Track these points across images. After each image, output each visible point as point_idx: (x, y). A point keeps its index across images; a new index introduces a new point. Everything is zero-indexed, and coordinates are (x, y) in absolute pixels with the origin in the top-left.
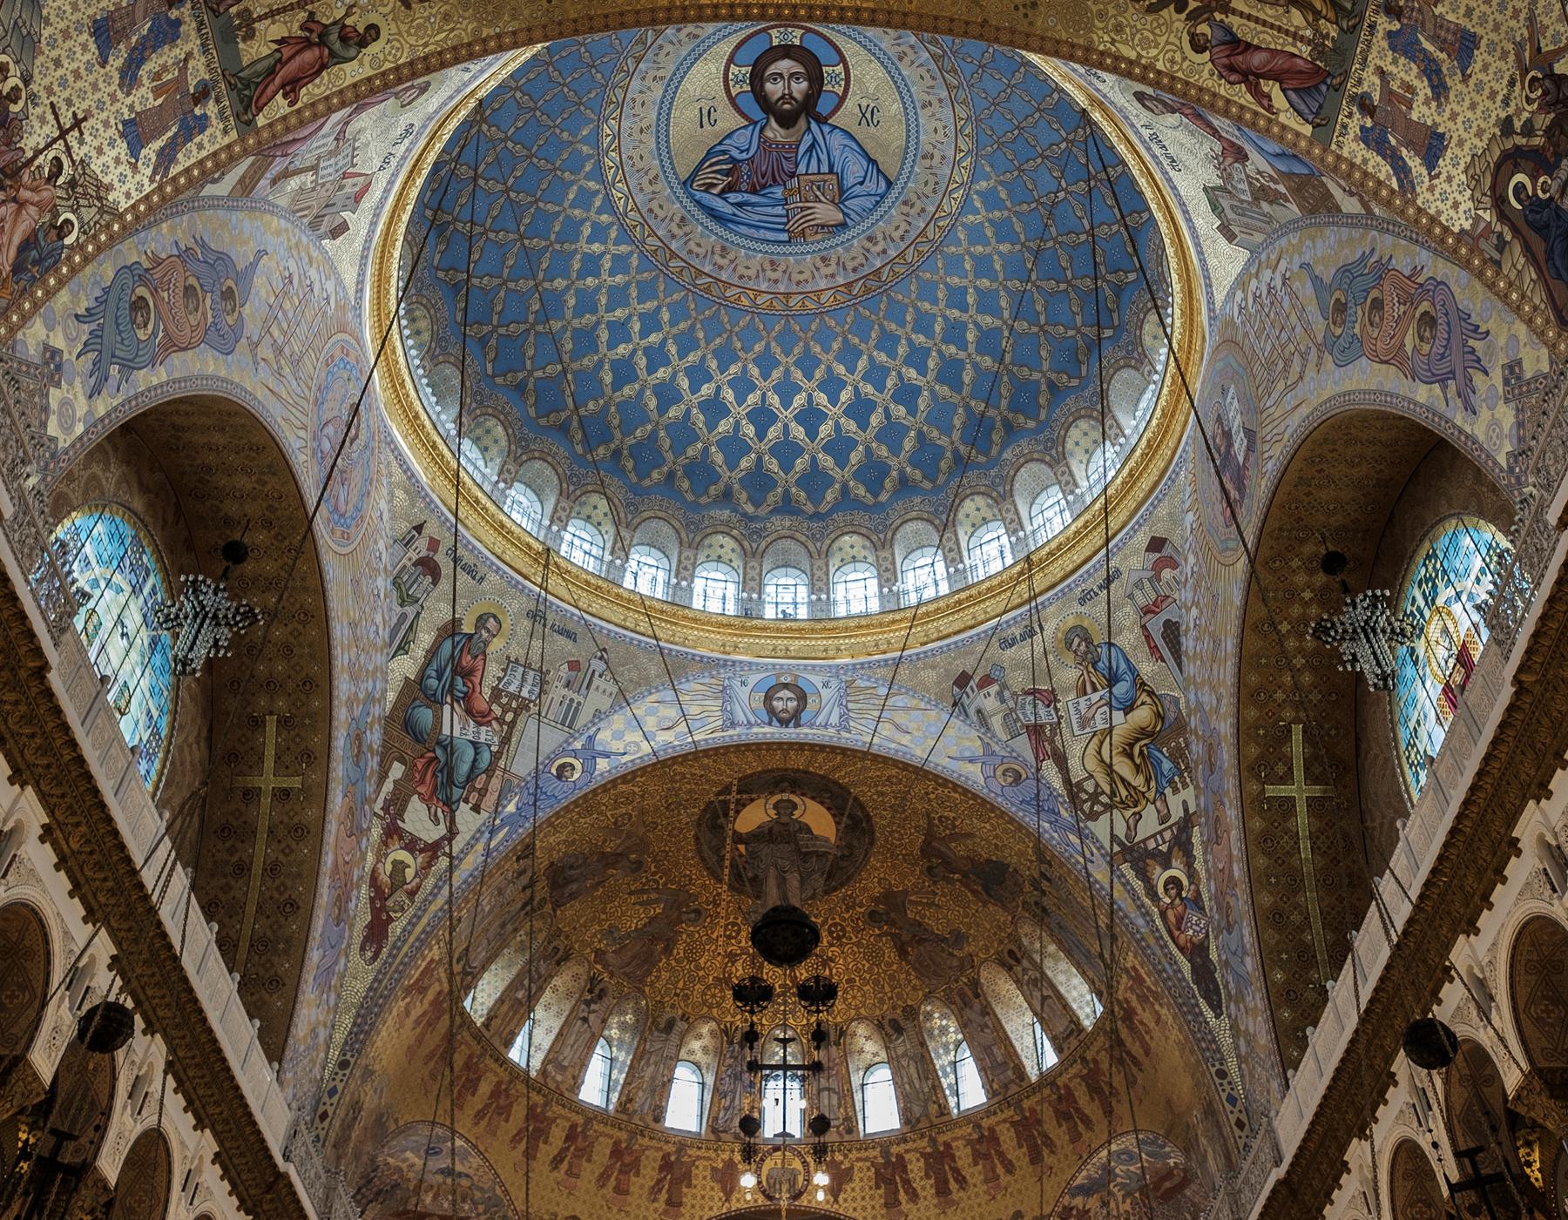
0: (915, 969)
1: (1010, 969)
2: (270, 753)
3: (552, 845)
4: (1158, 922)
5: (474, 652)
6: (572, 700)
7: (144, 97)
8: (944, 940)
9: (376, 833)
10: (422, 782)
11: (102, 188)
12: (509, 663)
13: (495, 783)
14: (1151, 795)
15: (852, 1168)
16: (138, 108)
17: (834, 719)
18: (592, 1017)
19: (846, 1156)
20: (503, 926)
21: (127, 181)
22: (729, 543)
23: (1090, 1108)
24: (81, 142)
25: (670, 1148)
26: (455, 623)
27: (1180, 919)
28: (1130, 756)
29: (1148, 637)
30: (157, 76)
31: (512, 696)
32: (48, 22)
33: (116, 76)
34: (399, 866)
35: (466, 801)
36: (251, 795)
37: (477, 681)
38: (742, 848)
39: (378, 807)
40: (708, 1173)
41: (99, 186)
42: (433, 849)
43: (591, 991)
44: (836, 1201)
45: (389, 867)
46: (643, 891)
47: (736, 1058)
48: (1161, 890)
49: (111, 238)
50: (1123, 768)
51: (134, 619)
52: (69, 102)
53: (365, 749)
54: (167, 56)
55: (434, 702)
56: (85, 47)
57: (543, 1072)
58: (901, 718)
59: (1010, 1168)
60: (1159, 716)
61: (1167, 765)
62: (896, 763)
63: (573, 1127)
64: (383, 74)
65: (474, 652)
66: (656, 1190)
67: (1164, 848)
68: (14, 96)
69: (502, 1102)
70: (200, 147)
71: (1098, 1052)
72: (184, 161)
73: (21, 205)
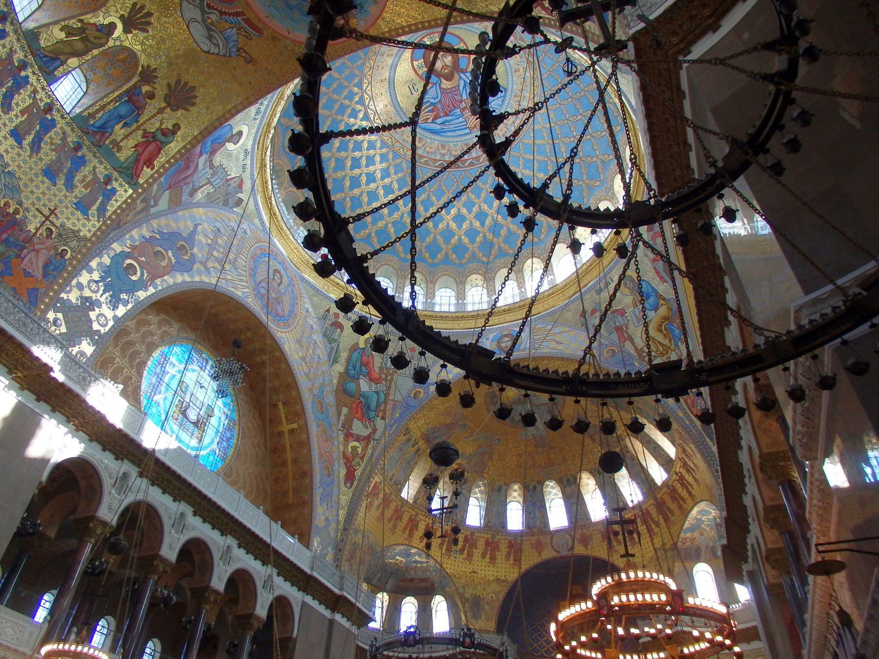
2: (283, 416)
4: (685, 406)
5: (367, 354)
7: (80, 190)
9: (342, 437)
10: (357, 413)
11: (75, 234)
13: (389, 406)
14: (672, 347)
16: (80, 196)
17: (528, 346)
20: (409, 462)
21: (88, 226)
22: (480, 277)
24: (57, 218)
25: (511, 538)
26: (357, 344)
27: (693, 402)
28: (661, 331)
29: (657, 273)
30: (83, 181)
32: (20, 179)
33: (63, 188)
34: (354, 448)
36: (281, 434)
39: (340, 427)
41: (73, 232)
42: (368, 439)
45: (350, 450)
49: (88, 249)
51: (206, 378)
52: (45, 205)
53: (324, 405)
54: (86, 170)
55: (356, 379)
56: (43, 182)
58: (557, 338)
59: (657, 524)
60: (670, 309)
62: (558, 359)
64: (190, 142)
65: (367, 354)
68: (17, 212)
70: (116, 201)
71: (678, 468)
72: (111, 209)
73: (38, 251)
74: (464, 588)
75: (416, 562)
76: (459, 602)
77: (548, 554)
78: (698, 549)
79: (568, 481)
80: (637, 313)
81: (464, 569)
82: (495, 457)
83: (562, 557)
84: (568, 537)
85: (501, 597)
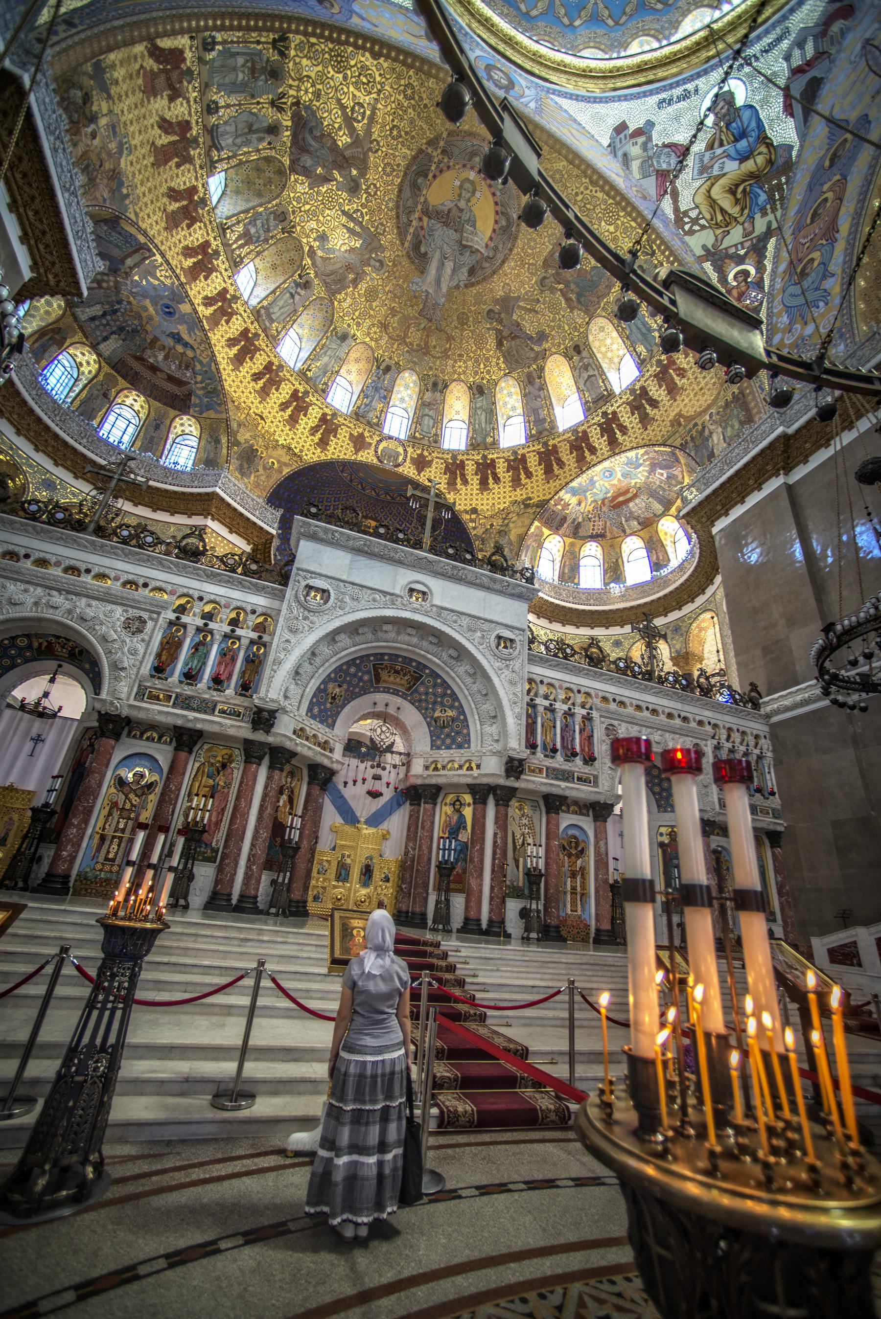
1: (569, 358)
8: (531, 338)
14: (741, 220)
15: (431, 462)
18: (297, 297)
23: (600, 442)
38: (425, 219)
48: (731, 277)
50: (726, 202)
61: (763, 197)
66: (314, 430)
67: (742, 252)
74: (239, 425)
76: (224, 440)
77: (367, 456)
78: (564, 519)
79: (435, 385)
80: (706, 159)
81: (248, 403)
82: (363, 287)
84: (401, 450)
85: (286, 471)
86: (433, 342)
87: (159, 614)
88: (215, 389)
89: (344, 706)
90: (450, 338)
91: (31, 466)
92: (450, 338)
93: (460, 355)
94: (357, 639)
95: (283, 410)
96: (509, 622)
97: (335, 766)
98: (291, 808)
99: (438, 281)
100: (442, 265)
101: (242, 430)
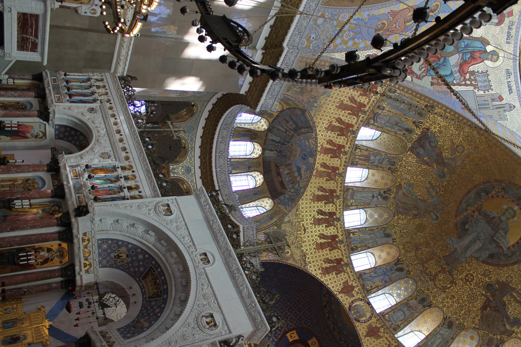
0: (482, 317)
3: (436, 124)
5: (482, 56)
6: (489, 104)
12: (486, 73)
15: (382, 337)
18: (375, 199)
19: (384, 333)
31: (476, 81)
35: (433, 78)
37: (472, 63)
38: (477, 213)
40: (344, 280)
43: (385, 192)
44: (365, 337)
46: (433, 187)
47: (391, 270)
57: (348, 188)
63: (334, 214)
69: (332, 174)
74: (289, 222)
75: (299, 170)
76: (275, 220)
77: (344, 300)
79: (423, 300)
82: (417, 221)
83: (347, 315)
84: (368, 315)
85: (291, 262)
86: (441, 277)
87: (116, 161)
88: (294, 199)
89: (118, 267)
90: (453, 282)
91: (191, 159)
92: (453, 282)
93: (453, 297)
94: (158, 244)
95: (320, 238)
96: (228, 320)
97: (78, 278)
98: (42, 263)
99: (467, 248)
100: (474, 242)
101: (288, 224)
